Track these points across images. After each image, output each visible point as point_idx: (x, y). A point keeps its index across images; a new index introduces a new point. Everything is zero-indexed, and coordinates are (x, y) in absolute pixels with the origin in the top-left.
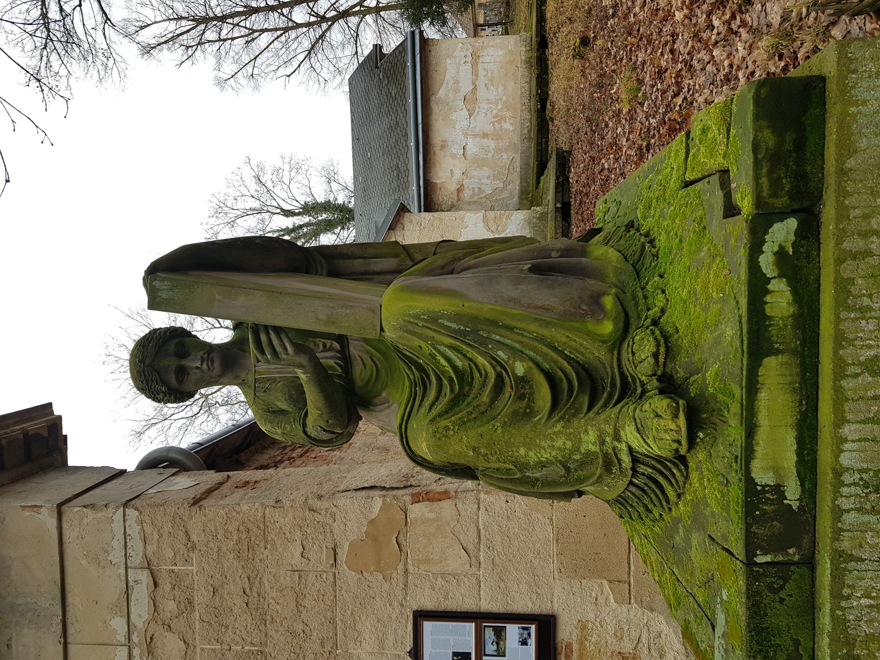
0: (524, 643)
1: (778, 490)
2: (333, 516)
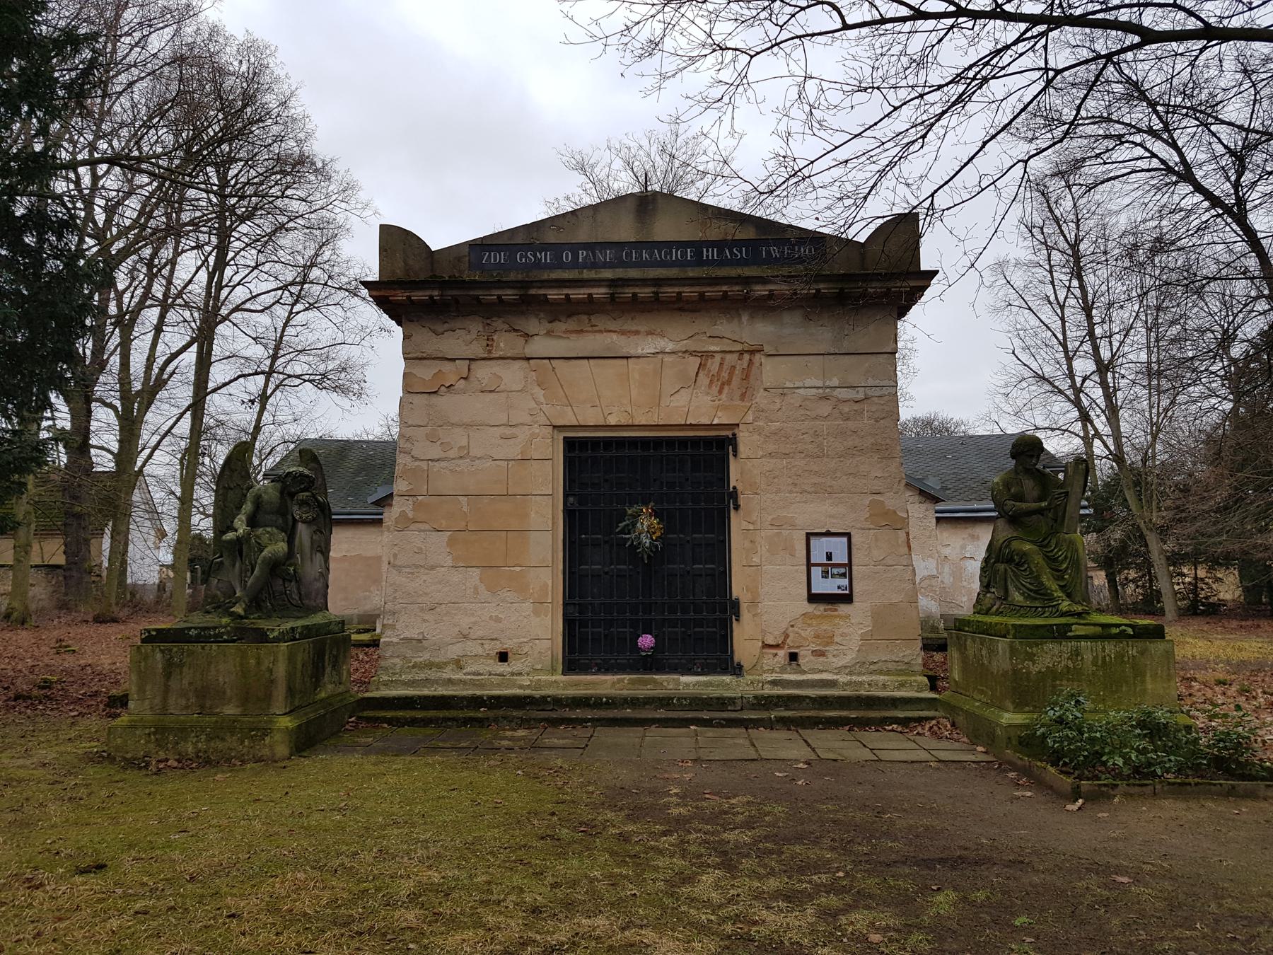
0: (839, 587)
1: (1071, 631)
2: (897, 493)
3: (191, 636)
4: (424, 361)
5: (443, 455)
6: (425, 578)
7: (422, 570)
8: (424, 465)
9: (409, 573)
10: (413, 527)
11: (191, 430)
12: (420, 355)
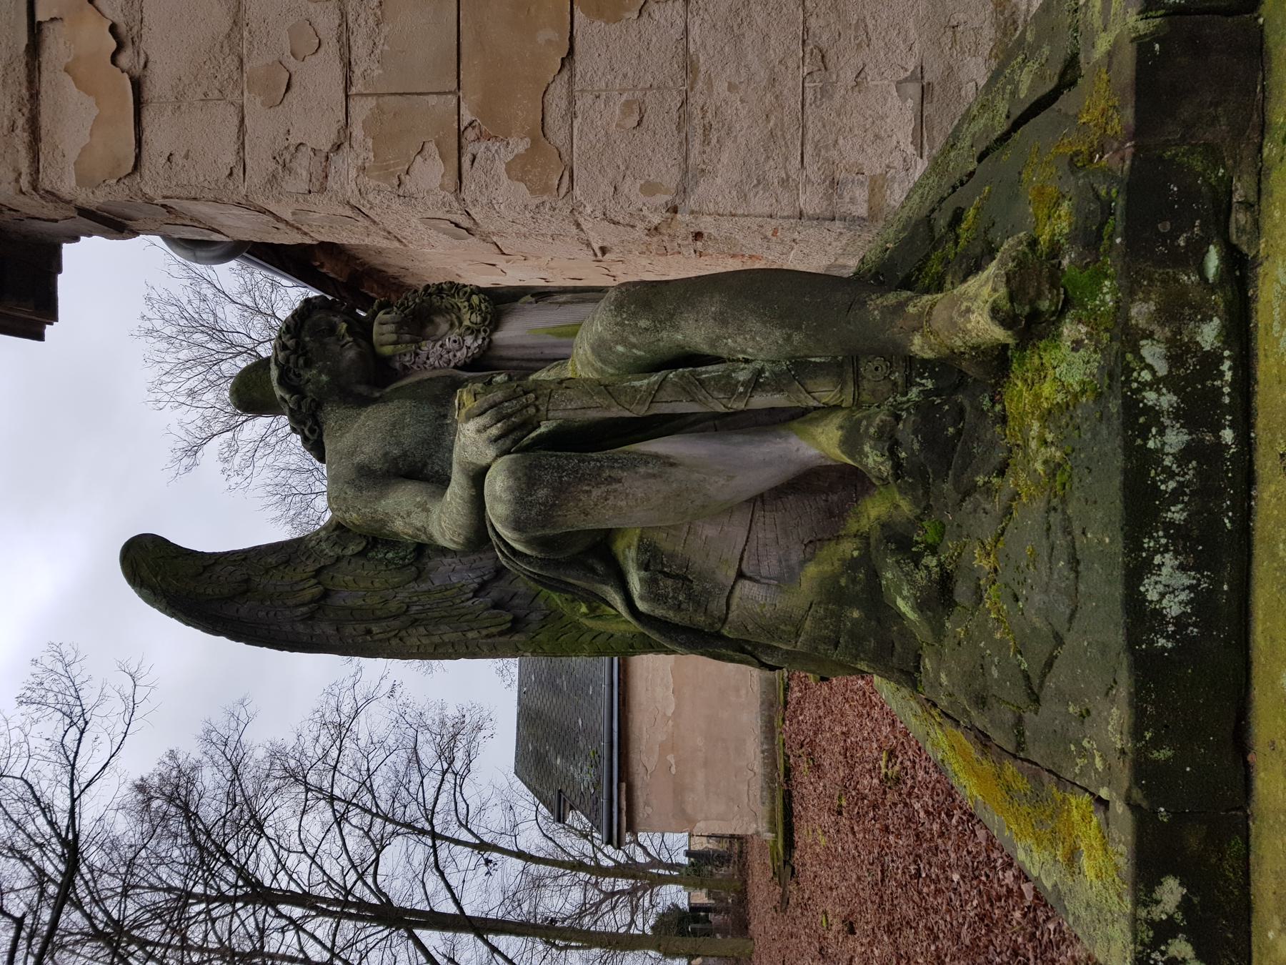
3: (1201, 602)
4: (45, 121)
5: (331, 48)
6: (721, 87)
7: (697, 100)
8: (362, 109)
9: (706, 141)
10: (558, 135)
11: (518, 934)
12: (22, 136)
